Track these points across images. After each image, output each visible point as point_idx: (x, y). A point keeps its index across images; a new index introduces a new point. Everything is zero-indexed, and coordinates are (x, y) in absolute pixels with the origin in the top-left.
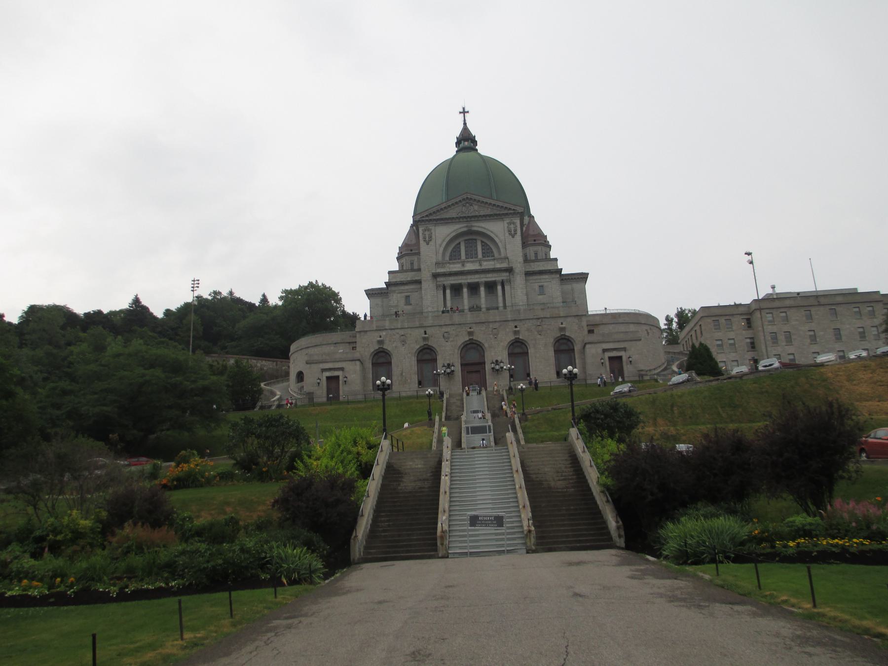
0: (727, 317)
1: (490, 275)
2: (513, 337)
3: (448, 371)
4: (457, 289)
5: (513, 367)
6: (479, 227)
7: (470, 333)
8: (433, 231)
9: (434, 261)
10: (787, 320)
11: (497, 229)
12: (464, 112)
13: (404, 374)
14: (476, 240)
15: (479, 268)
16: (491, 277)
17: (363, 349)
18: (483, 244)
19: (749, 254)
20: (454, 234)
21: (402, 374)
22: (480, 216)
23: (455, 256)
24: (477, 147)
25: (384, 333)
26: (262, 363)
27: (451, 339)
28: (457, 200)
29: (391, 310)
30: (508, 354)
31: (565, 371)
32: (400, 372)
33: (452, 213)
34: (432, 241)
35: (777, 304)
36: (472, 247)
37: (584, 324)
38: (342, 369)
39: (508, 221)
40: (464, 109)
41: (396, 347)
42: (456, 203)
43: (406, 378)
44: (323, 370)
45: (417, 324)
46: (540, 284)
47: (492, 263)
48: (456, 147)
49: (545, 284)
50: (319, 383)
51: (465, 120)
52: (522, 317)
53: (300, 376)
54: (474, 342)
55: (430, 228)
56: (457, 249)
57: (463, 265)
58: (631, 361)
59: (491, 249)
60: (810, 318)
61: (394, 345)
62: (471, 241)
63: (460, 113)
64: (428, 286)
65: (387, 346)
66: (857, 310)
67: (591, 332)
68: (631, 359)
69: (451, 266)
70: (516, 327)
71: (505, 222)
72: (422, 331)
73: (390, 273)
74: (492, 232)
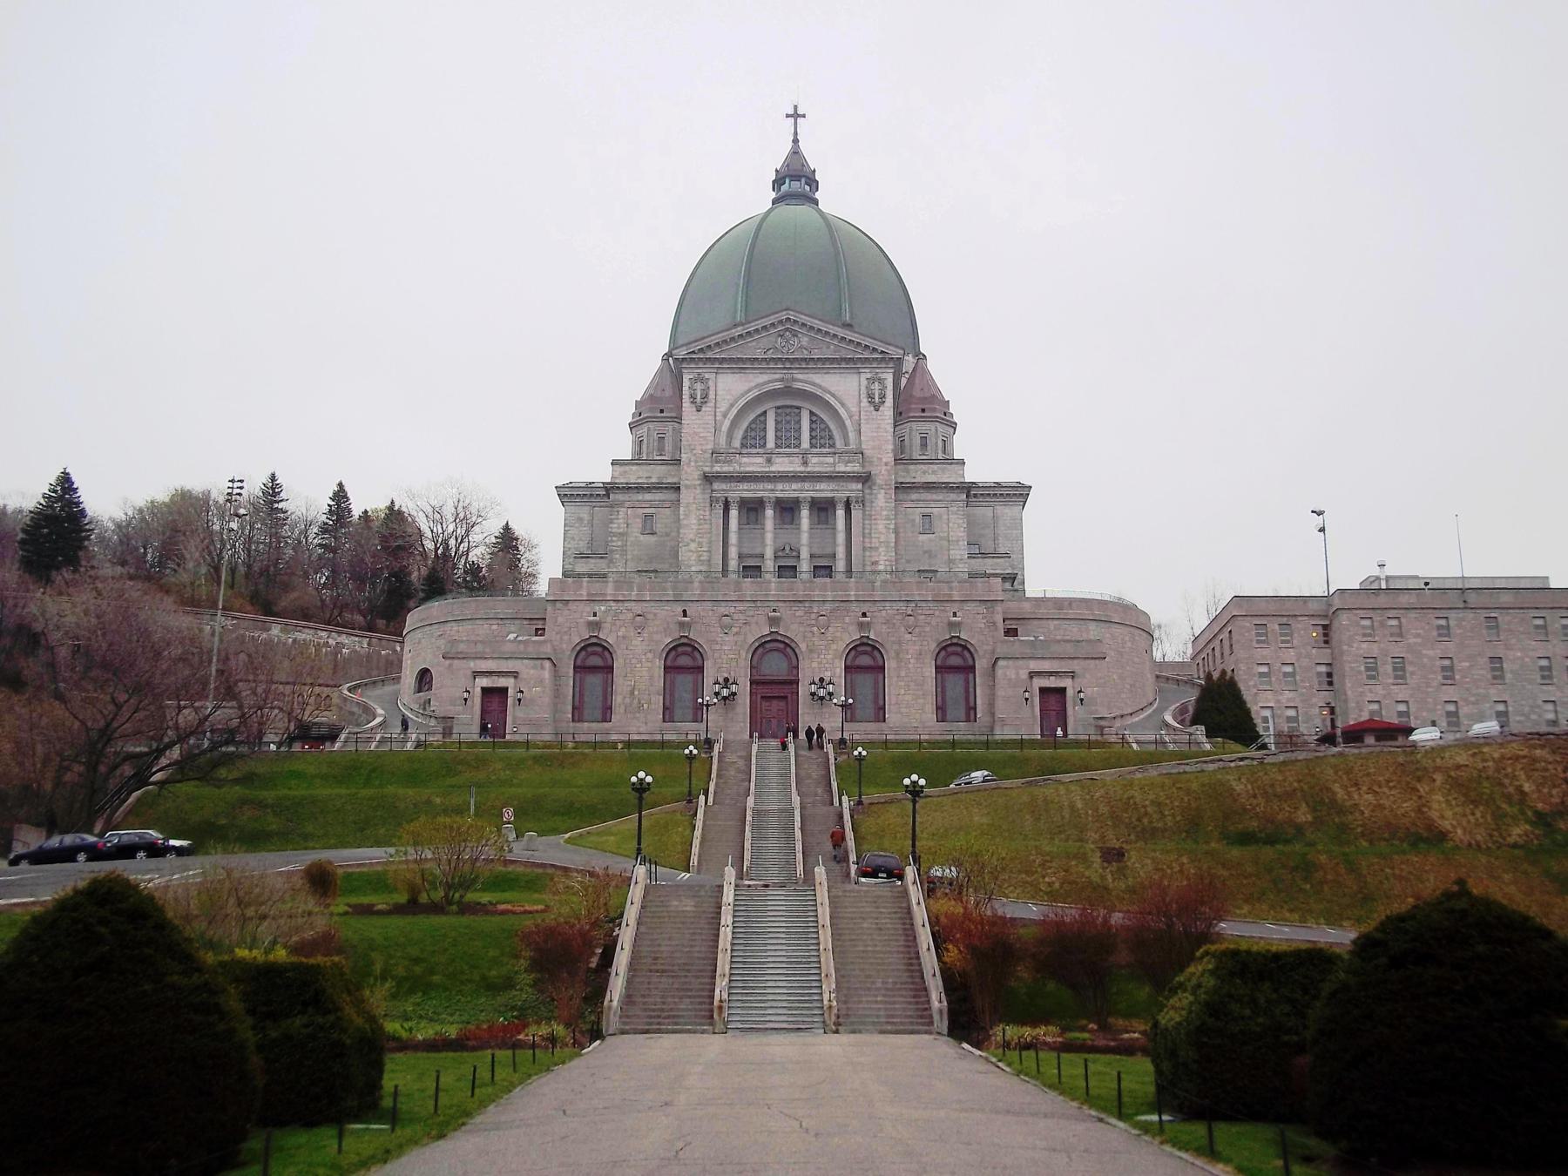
0: (1284, 620)
1: (823, 486)
3: (725, 692)
4: (752, 509)
5: (850, 701)
7: (773, 621)
8: (711, 383)
9: (710, 446)
10: (1400, 633)
11: (844, 388)
12: (796, 115)
13: (636, 693)
15: (802, 469)
16: (824, 490)
17: (558, 636)
18: (814, 418)
19: (1320, 513)
20: (756, 393)
21: (632, 693)
23: (754, 438)
24: (817, 195)
26: (339, 639)
27: (734, 630)
28: (767, 322)
29: (612, 541)
30: (846, 667)
31: (907, 781)
32: (629, 688)
33: (755, 349)
34: (708, 404)
35: (1382, 601)
36: (788, 422)
37: (999, 618)
38: (515, 675)
39: (869, 376)
40: (796, 107)
41: (624, 637)
42: (765, 328)
44: (477, 674)
45: (670, 594)
47: (831, 460)
48: (774, 190)
50: (466, 700)
51: (796, 133)
52: (878, 595)
53: (424, 678)
54: (779, 638)
55: (707, 376)
57: (769, 461)
58: (1082, 700)
59: (830, 431)
60: (1445, 632)
62: (788, 411)
63: (788, 116)
64: (693, 497)
65: (608, 636)
66: (1539, 622)
71: (863, 377)
72: (680, 609)
73: (614, 463)
74: (833, 395)
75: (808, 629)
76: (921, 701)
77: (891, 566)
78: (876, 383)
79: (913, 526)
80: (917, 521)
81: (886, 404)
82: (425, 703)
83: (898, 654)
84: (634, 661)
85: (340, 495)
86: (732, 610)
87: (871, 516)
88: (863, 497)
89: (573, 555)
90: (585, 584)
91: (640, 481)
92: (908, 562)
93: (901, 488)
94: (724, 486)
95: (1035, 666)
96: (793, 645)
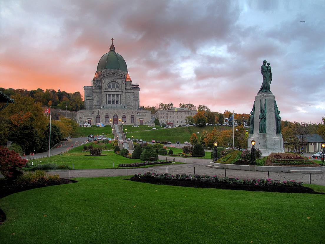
10: (173, 114)
12: (112, 40)
16: (117, 93)
23: (109, 87)
56: (110, 85)
64: (103, 93)
67: (138, 114)
85: (59, 90)
89: (86, 97)
93: (126, 93)
94: (107, 92)
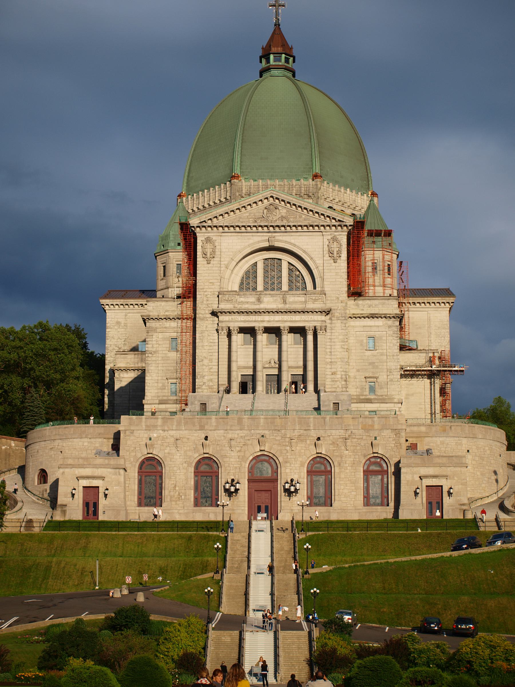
2: (312, 453)
6: (286, 242)
8: (216, 244)
13: (177, 488)
14: (280, 260)
16: (298, 321)
17: (128, 453)
22: (289, 226)
25: (155, 435)
31: (312, 591)
32: (173, 486)
34: (215, 259)
38: (103, 478)
39: (329, 237)
41: (169, 453)
43: (179, 494)
46: (372, 334)
49: (377, 334)
54: (266, 453)
55: (214, 238)
57: (259, 300)
61: (166, 451)
68: (451, 491)
69: (242, 299)
70: (319, 439)
72: (204, 436)
74: (304, 252)
75: (283, 448)
76: (353, 493)
77: (346, 375)
78: (335, 243)
79: (361, 345)
80: (365, 341)
81: (342, 258)
82: (43, 491)
83: (339, 464)
84: (175, 469)
86: (236, 436)
87: (331, 339)
88: (326, 326)
90: (144, 420)
91: (167, 313)
92: (358, 371)
95: (424, 471)
96: (274, 458)
